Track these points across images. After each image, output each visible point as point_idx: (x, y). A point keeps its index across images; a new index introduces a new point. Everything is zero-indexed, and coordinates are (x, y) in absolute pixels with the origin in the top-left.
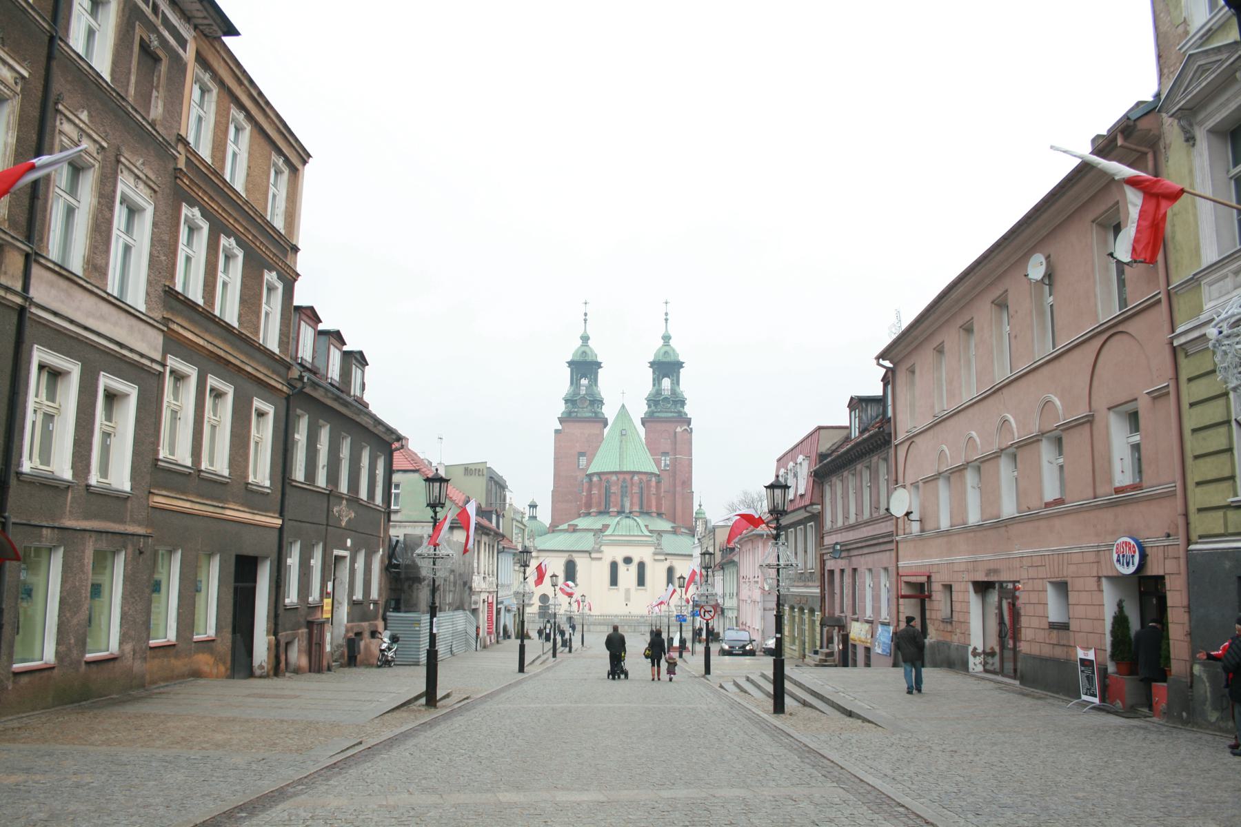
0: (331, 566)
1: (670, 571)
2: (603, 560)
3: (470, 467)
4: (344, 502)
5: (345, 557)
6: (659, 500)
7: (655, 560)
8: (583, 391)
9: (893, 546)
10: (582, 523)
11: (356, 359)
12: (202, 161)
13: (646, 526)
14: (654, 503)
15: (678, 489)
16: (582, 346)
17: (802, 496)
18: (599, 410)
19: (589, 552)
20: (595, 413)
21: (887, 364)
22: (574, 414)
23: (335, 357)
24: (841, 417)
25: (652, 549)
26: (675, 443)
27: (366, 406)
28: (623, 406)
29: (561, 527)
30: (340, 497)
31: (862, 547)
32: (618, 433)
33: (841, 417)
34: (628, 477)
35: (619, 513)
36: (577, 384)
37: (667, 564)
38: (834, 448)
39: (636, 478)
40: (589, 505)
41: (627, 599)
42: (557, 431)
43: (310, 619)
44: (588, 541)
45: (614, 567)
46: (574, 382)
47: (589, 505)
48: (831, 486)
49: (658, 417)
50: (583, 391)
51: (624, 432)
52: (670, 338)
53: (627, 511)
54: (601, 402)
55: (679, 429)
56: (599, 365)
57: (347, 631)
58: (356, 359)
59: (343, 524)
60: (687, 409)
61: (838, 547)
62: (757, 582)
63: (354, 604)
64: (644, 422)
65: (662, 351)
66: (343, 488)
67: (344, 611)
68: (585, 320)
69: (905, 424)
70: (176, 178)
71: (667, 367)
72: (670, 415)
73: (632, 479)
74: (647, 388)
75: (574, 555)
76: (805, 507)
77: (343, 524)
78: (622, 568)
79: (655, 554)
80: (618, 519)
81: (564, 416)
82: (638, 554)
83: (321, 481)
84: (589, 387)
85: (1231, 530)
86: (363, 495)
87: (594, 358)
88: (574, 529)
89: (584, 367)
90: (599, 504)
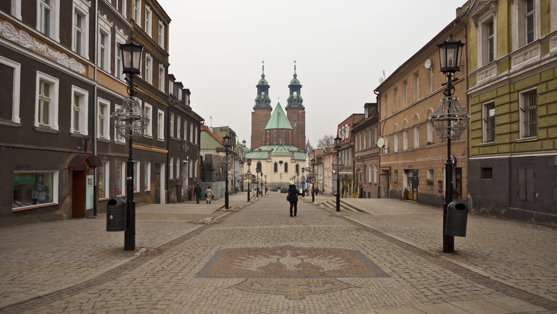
0: (182, 165)
1: (297, 166)
2: (272, 162)
3: (222, 128)
4: (186, 144)
5: (187, 163)
6: (292, 139)
7: (292, 162)
8: (263, 97)
9: (378, 157)
10: (263, 148)
11: (187, 92)
12: (138, 27)
13: (288, 149)
14: (291, 140)
15: (300, 135)
17: (347, 139)
18: (269, 104)
19: (266, 159)
20: (267, 105)
21: (378, 93)
22: (259, 106)
23: (180, 92)
24: (361, 110)
25: (290, 158)
26: (298, 117)
27: (191, 108)
28: (279, 103)
29: (255, 150)
30: (184, 142)
31: (368, 158)
32: (277, 114)
33: (361, 110)
34: (281, 131)
35: (277, 145)
36: (260, 94)
37: (296, 163)
38: (359, 122)
39: (284, 131)
40: (266, 142)
41: (281, 177)
42: (252, 113)
43: (177, 184)
44: (266, 155)
45: (276, 165)
46: (259, 93)
47: (266, 142)
48: (357, 135)
49: (292, 107)
50: (263, 97)
51: (279, 113)
52: (296, 76)
53: (280, 144)
54: (270, 101)
55: (300, 112)
56: (269, 87)
57: (188, 188)
58: (187, 92)
59: (186, 151)
60: (303, 104)
61: (360, 158)
62: (330, 170)
63: (189, 179)
64: (286, 109)
65: (293, 81)
66: (185, 139)
67: (186, 182)
68: (263, 69)
69: (384, 114)
70: (131, 34)
71: (295, 87)
72: (297, 106)
73: (282, 131)
74: (288, 95)
75: (261, 160)
76: (348, 143)
77: (186, 151)
78: (279, 165)
79: (291, 160)
80: (277, 147)
82: (285, 160)
83: (179, 136)
84: (265, 96)
85: (480, 154)
86: (191, 141)
87: (267, 84)
88: (260, 151)
89: (263, 87)
90: (270, 141)
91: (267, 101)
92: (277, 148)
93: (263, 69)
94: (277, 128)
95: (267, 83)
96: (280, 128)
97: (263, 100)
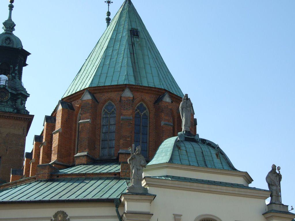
16: (6, 33)
32: (125, 34)
90: (92, 146)
91: (18, 94)
92: (177, 146)
94: (132, 82)
95: (22, 47)
96: (145, 84)
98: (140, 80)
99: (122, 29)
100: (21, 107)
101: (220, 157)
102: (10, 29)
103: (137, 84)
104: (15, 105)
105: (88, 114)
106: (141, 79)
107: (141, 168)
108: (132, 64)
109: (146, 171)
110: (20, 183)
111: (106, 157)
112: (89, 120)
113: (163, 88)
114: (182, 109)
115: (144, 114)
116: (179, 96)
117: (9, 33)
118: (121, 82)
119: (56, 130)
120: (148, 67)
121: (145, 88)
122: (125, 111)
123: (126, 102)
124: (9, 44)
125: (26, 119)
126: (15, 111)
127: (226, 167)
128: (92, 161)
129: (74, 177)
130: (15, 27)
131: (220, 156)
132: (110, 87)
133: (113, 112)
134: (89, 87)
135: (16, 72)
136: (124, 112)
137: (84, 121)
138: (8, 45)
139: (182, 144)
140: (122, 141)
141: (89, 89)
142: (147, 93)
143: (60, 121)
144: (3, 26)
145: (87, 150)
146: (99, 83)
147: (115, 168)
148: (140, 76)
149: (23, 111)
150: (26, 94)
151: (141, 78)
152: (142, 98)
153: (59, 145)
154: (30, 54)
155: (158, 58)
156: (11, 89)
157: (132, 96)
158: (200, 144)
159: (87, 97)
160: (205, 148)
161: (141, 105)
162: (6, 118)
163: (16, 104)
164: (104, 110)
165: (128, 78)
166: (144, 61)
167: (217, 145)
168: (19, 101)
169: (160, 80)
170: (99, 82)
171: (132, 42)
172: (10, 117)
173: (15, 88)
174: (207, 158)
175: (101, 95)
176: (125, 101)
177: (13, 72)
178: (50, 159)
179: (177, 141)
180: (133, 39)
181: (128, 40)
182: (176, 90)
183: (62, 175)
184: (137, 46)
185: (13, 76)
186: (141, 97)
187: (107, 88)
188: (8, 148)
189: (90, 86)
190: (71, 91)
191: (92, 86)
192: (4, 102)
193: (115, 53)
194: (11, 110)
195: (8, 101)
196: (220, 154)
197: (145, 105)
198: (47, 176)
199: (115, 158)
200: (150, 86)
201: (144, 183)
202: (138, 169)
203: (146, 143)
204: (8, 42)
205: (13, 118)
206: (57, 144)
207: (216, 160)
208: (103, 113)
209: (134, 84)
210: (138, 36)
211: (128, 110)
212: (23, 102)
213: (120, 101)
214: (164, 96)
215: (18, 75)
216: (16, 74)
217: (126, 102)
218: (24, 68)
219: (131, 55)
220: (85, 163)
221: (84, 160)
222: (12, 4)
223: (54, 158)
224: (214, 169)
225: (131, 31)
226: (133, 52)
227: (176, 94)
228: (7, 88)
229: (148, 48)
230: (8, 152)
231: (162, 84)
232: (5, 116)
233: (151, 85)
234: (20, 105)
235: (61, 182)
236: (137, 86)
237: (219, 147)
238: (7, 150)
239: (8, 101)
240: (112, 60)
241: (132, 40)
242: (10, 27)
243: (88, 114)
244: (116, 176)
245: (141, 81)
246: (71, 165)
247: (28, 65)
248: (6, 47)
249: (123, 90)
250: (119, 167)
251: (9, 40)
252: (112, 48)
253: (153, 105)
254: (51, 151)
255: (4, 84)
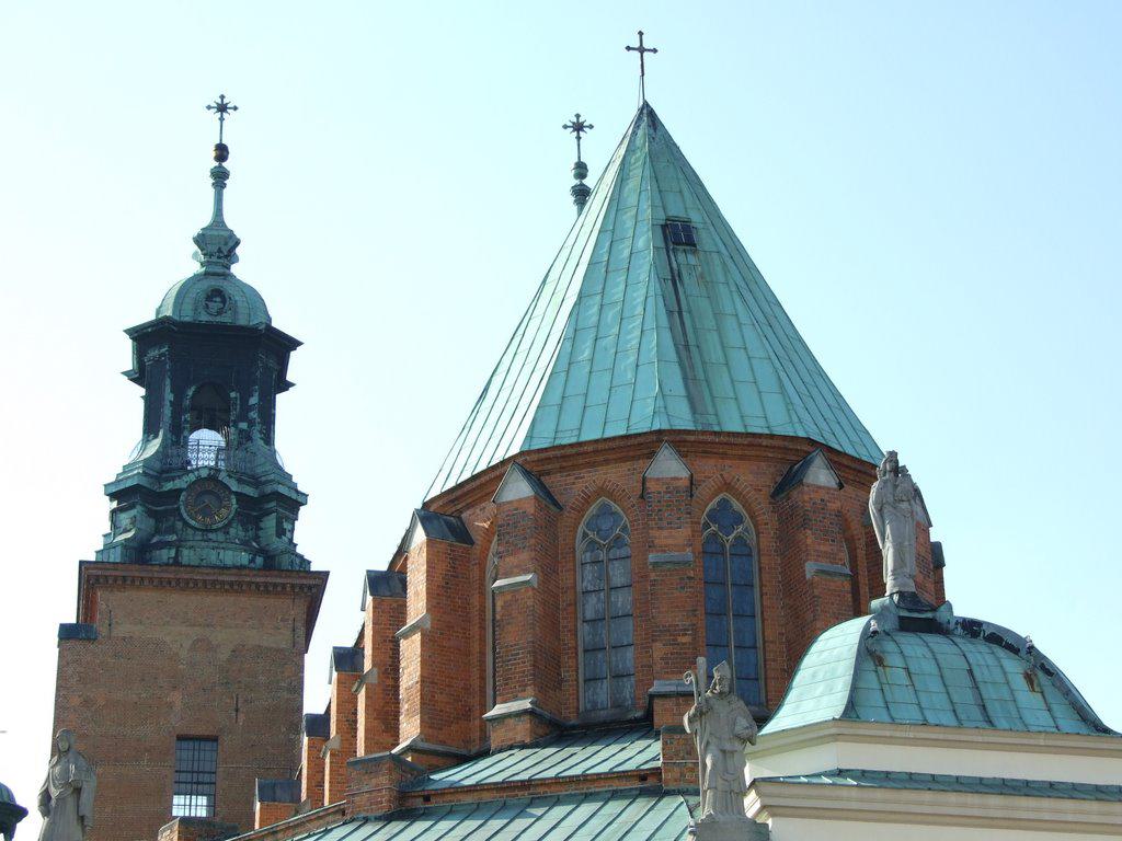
16: (206, 274)
20: (262, 551)
22: (166, 555)
32: (644, 242)
68: (220, 177)
81: (115, 556)
90: (548, 672)
91: (266, 498)
92: (870, 653)
93: (220, 177)
94: (683, 419)
97: (210, 483)
98: (711, 410)
99: (630, 224)
100: (277, 544)
101: (1039, 685)
102: (219, 258)
103: (700, 428)
104: (257, 538)
105: (525, 556)
106: (714, 406)
107: (737, 745)
108: (678, 352)
109: (755, 756)
110: (291, 832)
111: (603, 713)
112: (529, 577)
113: (801, 434)
114: (880, 511)
115: (739, 538)
116: (865, 458)
117: (218, 275)
118: (641, 425)
119: (411, 621)
120: (738, 358)
121: (732, 440)
122: (665, 533)
123: (667, 497)
124: (220, 312)
125: (301, 587)
126: (259, 560)
127: (1068, 722)
128: (555, 730)
129: (486, 796)
130: (238, 250)
131: (1042, 683)
132: (600, 447)
133: (618, 537)
134: (522, 453)
135: (254, 415)
136: (662, 537)
137: (513, 579)
138: (218, 319)
139: (890, 646)
140: (659, 650)
141: (520, 460)
142: (742, 458)
143: (422, 588)
144: (196, 248)
145: (530, 690)
146: (559, 435)
147: (640, 754)
148: (711, 394)
149: (285, 561)
150: (294, 496)
151: (713, 401)
152: (725, 476)
153: (423, 680)
154: (300, 344)
155: (773, 321)
156: (240, 481)
157: (684, 474)
158: (957, 640)
159: (518, 489)
160: (979, 653)
161: (724, 504)
162: (226, 591)
163: (260, 533)
164: (585, 535)
165: (665, 408)
166: (720, 337)
167: (1024, 641)
168: (270, 523)
169: (789, 404)
170: (560, 428)
171: (671, 268)
172: (240, 584)
173: (253, 477)
174: (989, 693)
175: (570, 479)
176: (659, 493)
177: (243, 417)
178: (393, 730)
179: (868, 636)
180: (672, 257)
181: (655, 264)
182: (854, 438)
183: (442, 793)
184: (689, 282)
185: (241, 431)
186: (721, 475)
187: (590, 448)
188: (240, 701)
189: (526, 448)
190: (456, 472)
191: (533, 448)
192: (216, 530)
193: (611, 315)
194: (244, 558)
195: (229, 524)
196: (1040, 674)
197: (737, 505)
198: (385, 802)
199: (639, 714)
200: (749, 431)
201: (751, 804)
202: (724, 752)
203: (755, 648)
204: (215, 306)
205: (253, 587)
206: (418, 673)
207: (1028, 699)
208: (580, 546)
209: (690, 427)
210: (695, 245)
211: (671, 528)
212: (287, 526)
213: (642, 497)
214: (807, 463)
215: (258, 427)
216: (251, 423)
217: (667, 497)
218: (281, 399)
219: (669, 321)
220: (527, 741)
221: (522, 730)
222: (224, 164)
223: (410, 729)
224: (1023, 735)
225: (664, 227)
226: (680, 308)
227: (850, 451)
228: (222, 476)
229: (734, 289)
230: (242, 717)
231: (795, 419)
232: (223, 583)
233: (757, 427)
234: (275, 539)
235: (440, 820)
236: (704, 433)
237: (1032, 647)
238: (237, 711)
239: (229, 524)
240: (602, 343)
241: (670, 264)
242: (220, 251)
243: (525, 556)
244: (648, 785)
245: (716, 415)
246: (474, 750)
247: (293, 385)
248: (209, 326)
249: (651, 455)
250: (656, 747)
251: (218, 299)
252: (598, 298)
253: (770, 503)
254: (397, 702)
255: (212, 464)
